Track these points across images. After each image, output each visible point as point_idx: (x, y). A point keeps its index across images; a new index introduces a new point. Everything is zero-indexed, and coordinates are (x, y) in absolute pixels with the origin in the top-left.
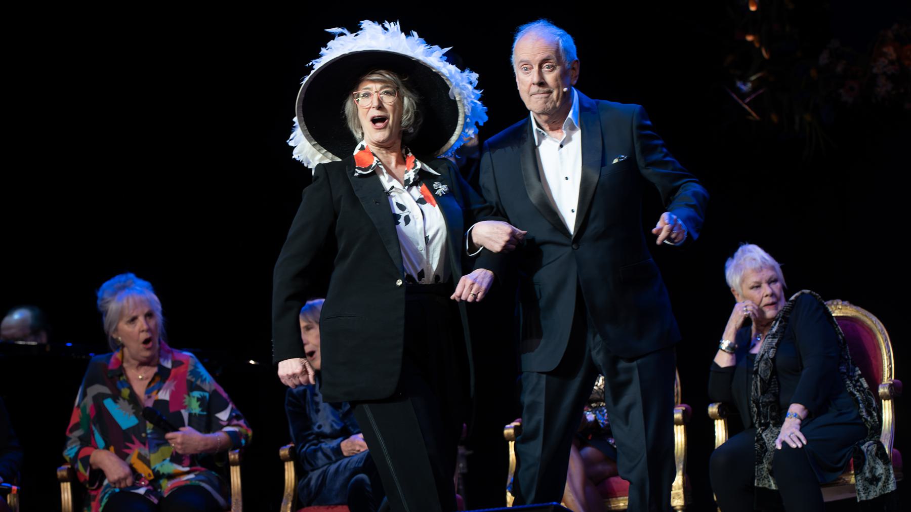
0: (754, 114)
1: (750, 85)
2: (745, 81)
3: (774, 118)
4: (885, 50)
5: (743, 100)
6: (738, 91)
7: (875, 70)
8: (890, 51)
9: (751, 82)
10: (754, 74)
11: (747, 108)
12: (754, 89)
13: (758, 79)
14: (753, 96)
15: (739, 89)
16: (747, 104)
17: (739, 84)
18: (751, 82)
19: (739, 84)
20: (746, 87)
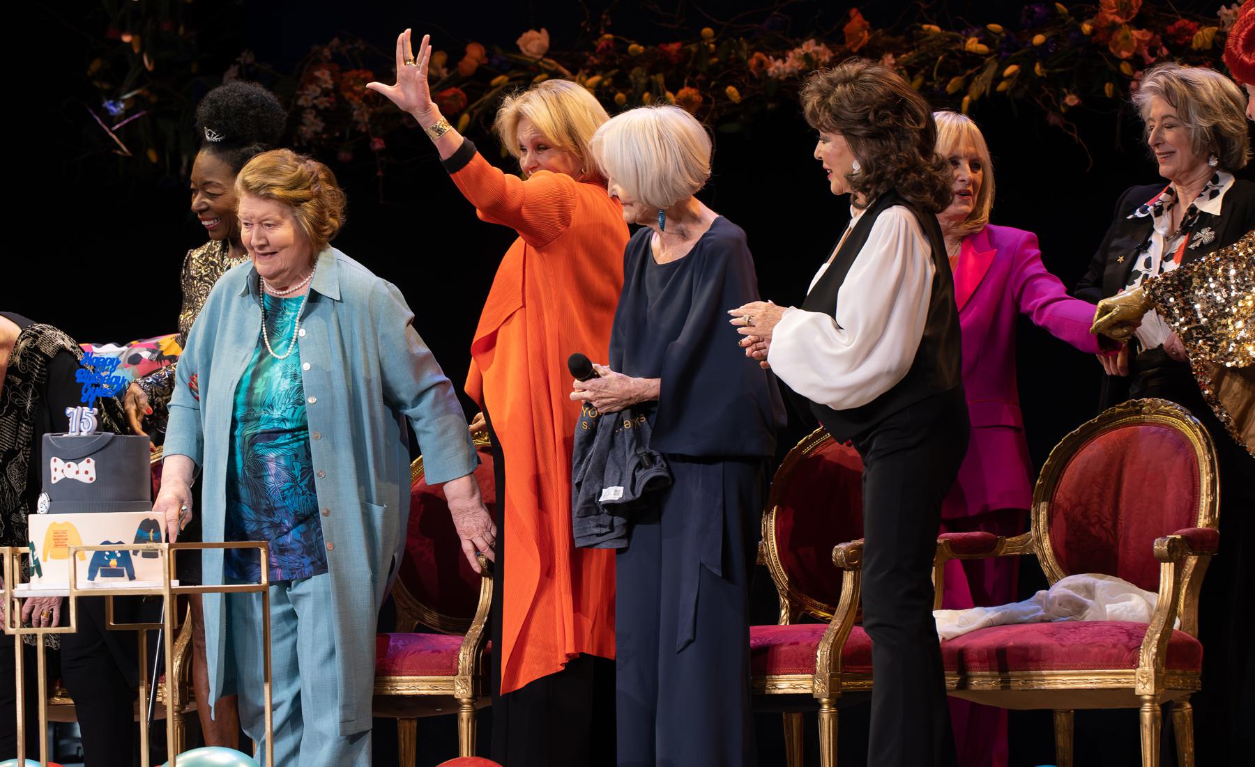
0: (124, 149)
1: (122, 106)
2: (116, 99)
3: (153, 156)
4: (317, 74)
5: (110, 126)
6: (105, 114)
7: (301, 102)
8: (325, 76)
9: (124, 101)
10: (129, 92)
11: (114, 137)
12: (127, 113)
13: (134, 97)
14: (125, 122)
15: (107, 111)
16: (114, 132)
17: (107, 104)
18: (124, 101)
19: (107, 104)
20: (117, 109)
